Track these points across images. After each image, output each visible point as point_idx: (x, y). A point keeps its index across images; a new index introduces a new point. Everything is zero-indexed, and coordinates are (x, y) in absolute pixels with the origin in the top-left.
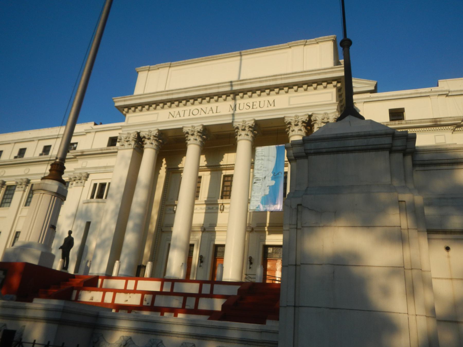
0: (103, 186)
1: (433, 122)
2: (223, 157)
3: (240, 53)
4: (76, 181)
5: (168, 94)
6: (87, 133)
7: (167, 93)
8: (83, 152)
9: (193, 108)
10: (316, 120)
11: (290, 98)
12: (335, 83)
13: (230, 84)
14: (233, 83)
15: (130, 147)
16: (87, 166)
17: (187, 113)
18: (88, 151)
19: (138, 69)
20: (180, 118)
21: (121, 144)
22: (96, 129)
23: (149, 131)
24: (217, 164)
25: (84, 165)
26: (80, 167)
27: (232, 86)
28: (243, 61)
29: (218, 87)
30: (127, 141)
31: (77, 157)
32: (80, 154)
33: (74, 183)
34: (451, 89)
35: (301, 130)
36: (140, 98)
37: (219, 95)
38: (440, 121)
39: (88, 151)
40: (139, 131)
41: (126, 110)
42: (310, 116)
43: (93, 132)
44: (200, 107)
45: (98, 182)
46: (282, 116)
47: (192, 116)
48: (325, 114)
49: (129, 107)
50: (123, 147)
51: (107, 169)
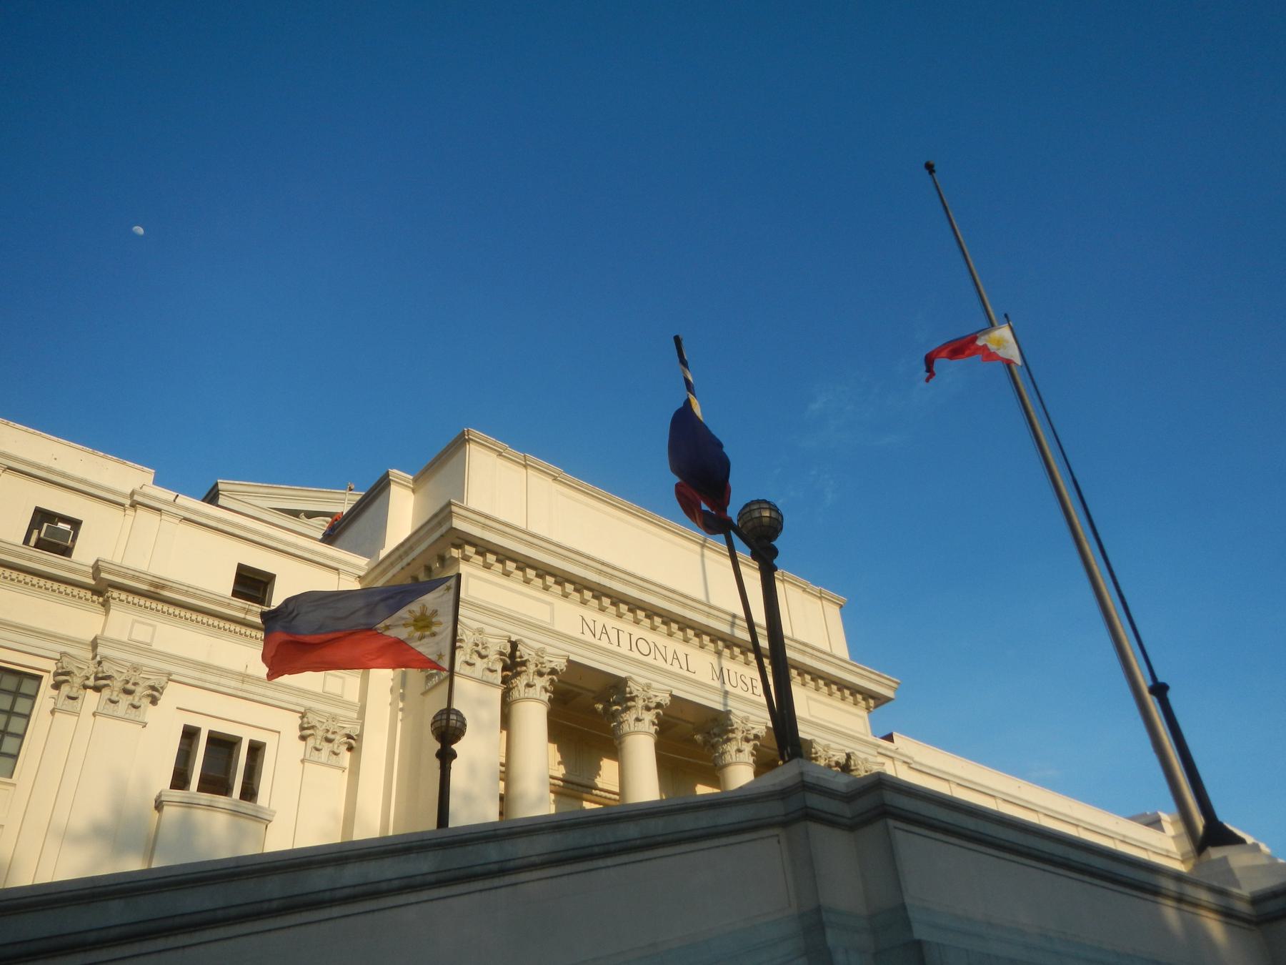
0: (222, 745)
2: (599, 768)
3: (705, 541)
4: (106, 693)
5: (600, 572)
6: (134, 505)
7: (600, 567)
8: (163, 587)
9: (638, 632)
11: (809, 698)
12: (872, 702)
13: (730, 618)
14: (738, 621)
16: (155, 647)
18: (186, 593)
19: (475, 433)
21: (463, 658)
22: (187, 509)
24: (585, 782)
25: (141, 634)
26: (125, 639)
27: (733, 625)
28: (706, 561)
31: (115, 594)
32: (145, 587)
33: (91, 698)
36: (531, 544)
37: (701, 631)
39: (186, 593)
41: (470, 550)
43: (175, 515)
44: (651, 637)
45: (206, 727)
47: (636, 655)
48: (866, 760)
49: (484, 548)
51: (246, 686)
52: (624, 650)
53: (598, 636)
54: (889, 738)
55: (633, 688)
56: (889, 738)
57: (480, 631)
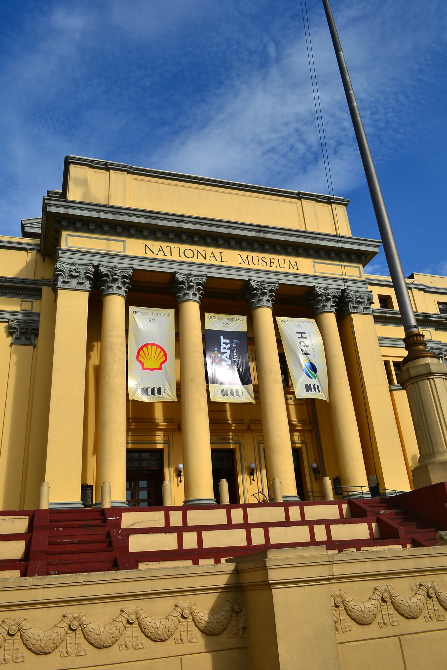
1: (422, 316)
9: (184, 247)
10: (351, 298)
15: (81, 287)
17: (175, 252)
20: (165, 258)
23: (115, 267)
29: (230, 227)
30: (75, 277)
34: (428, 285)
35: (332, 306)
36: (99, 211)
38: (429, 317)
40: (96, 263)
41: (64, 223)
42: (344, 291)
44: (194, 248)
46: (312, 285)
48: (358, 291)
50: (66, 286)
52: (175, 257)
53: (156, 253)
54: (412, 277)
55: (179, 277)
56: (412, 277)
57: (73, 264)
